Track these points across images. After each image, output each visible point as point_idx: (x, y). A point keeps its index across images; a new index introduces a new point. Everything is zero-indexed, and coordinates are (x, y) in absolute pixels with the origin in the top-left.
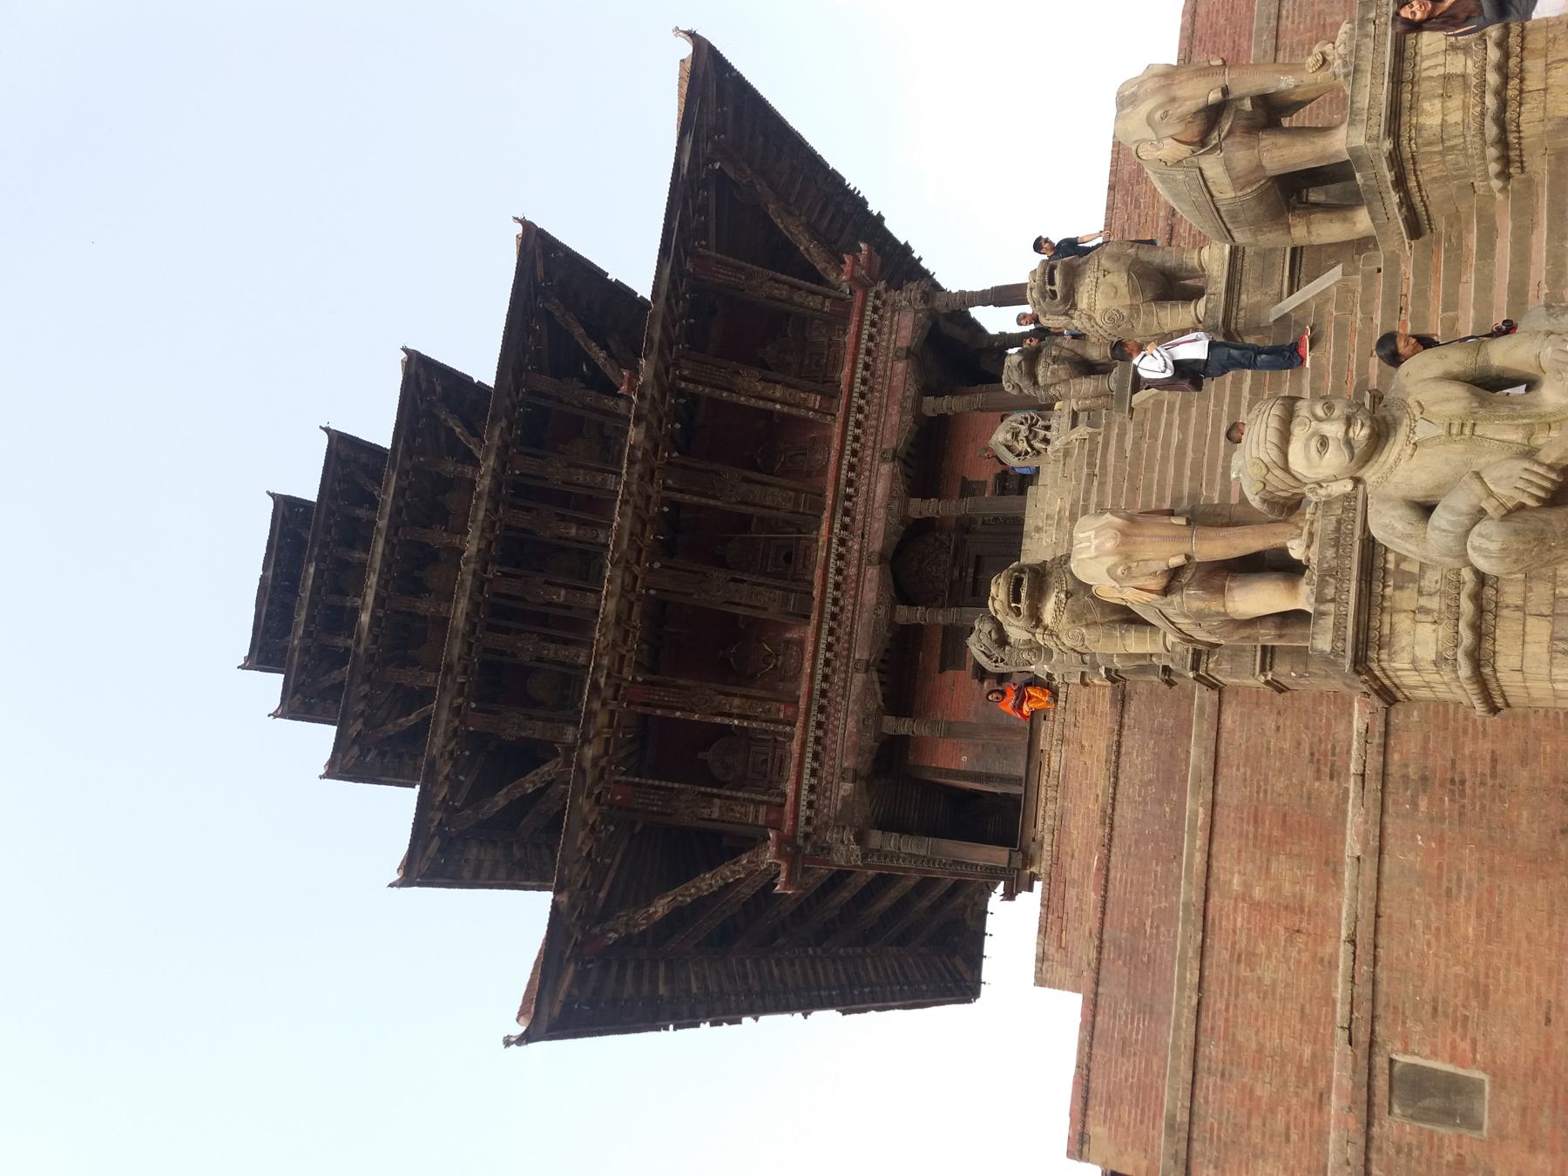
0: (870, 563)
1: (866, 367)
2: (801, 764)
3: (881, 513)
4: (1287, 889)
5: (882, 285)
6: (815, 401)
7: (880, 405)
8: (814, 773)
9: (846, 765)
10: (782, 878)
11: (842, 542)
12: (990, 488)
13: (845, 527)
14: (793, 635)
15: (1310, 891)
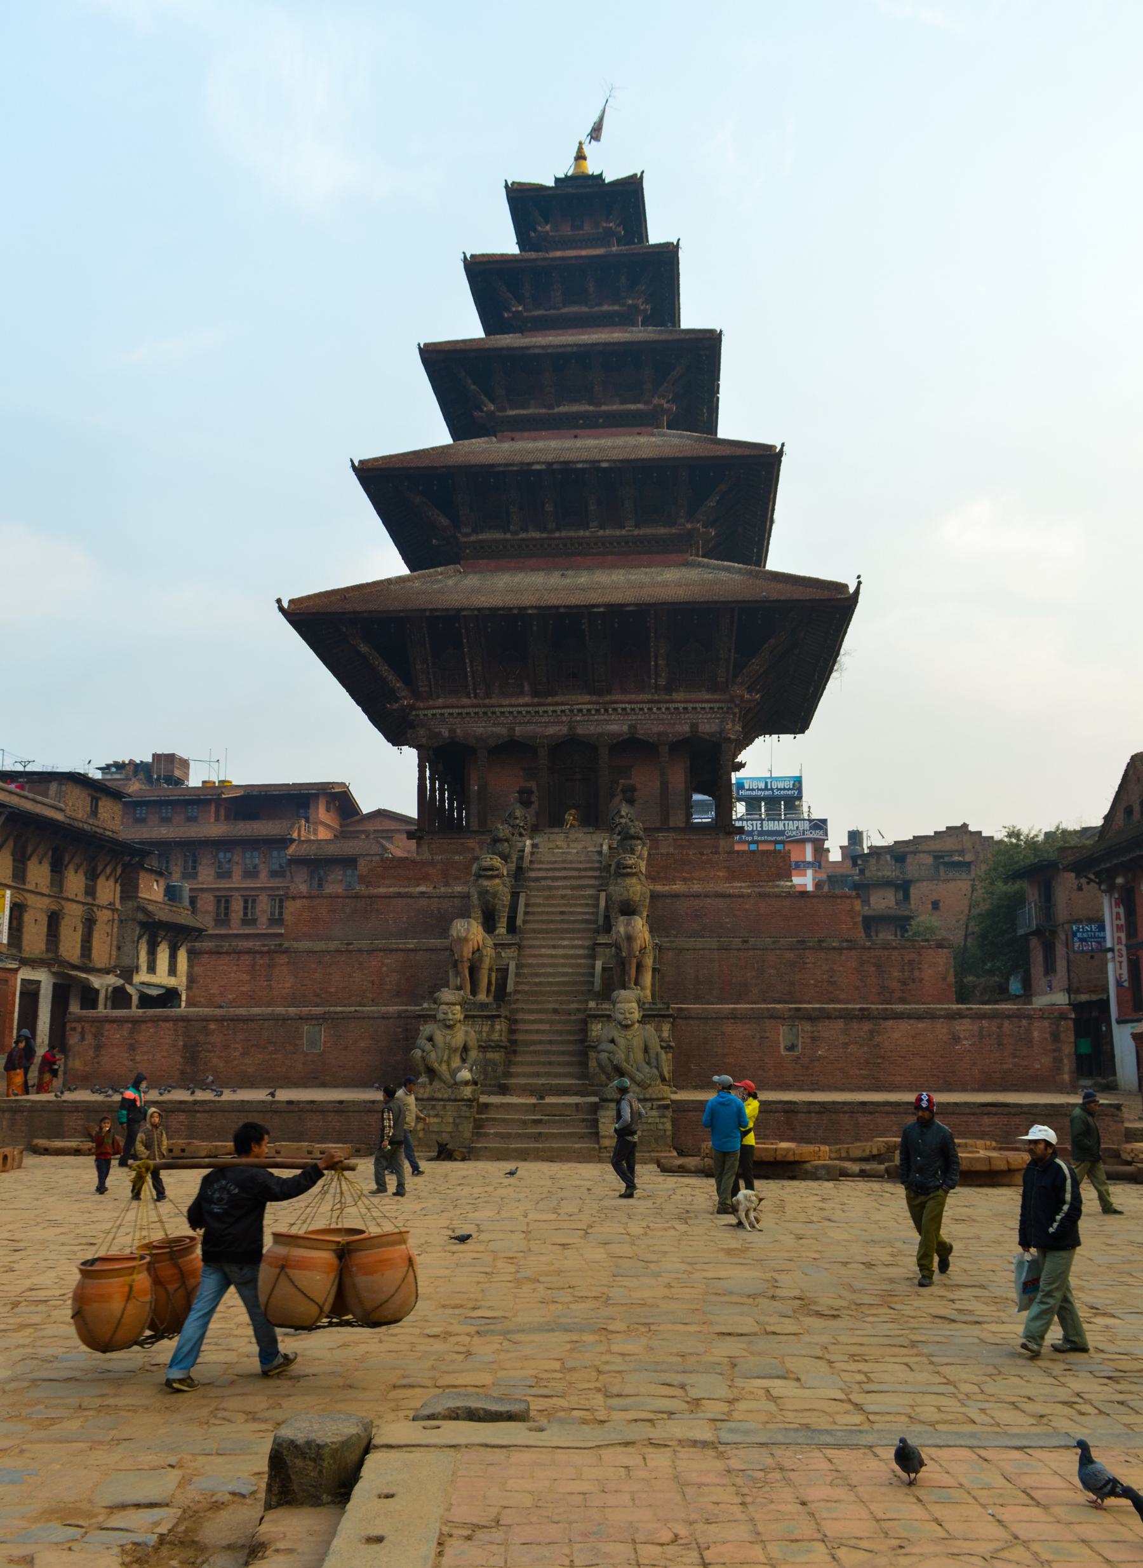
0: (570, 729)
1: (685, 708)
2: (453, 707)
3: (599, 730)
4: (387, 979)
5: (737, 710)
6: (662, 682)
7: (663, 719)
8: (450, 714)
9: (458, 731)
10: (396, 706)
11: (580, 711)
12: (628, 782)
13: (589, 710)
14: (526, 688)
15: (388, 987)
